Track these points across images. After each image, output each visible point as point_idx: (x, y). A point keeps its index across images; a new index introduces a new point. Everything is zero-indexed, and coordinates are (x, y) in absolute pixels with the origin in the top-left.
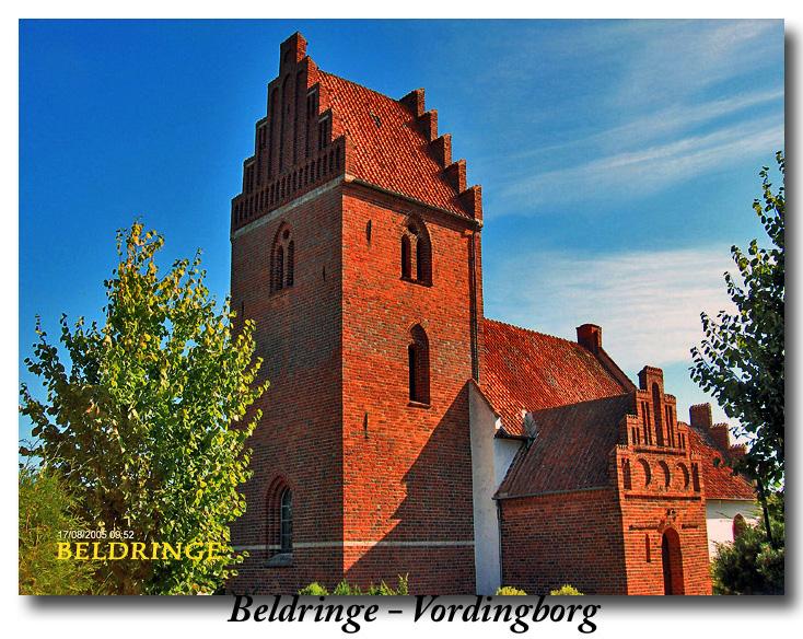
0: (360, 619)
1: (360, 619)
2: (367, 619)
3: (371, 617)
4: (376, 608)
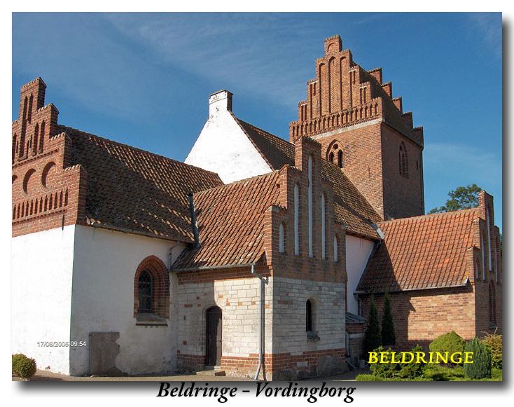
0: (227, 395)
1: (227, 395)
2: (231, 395)
3: (233, 394)
4: (236, 389)
